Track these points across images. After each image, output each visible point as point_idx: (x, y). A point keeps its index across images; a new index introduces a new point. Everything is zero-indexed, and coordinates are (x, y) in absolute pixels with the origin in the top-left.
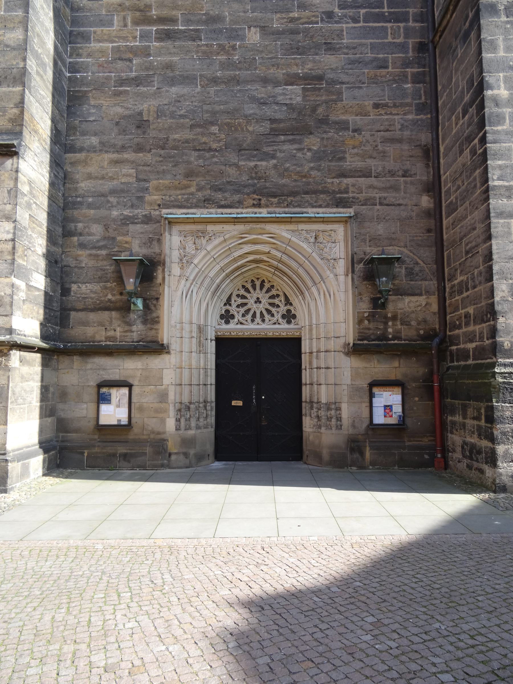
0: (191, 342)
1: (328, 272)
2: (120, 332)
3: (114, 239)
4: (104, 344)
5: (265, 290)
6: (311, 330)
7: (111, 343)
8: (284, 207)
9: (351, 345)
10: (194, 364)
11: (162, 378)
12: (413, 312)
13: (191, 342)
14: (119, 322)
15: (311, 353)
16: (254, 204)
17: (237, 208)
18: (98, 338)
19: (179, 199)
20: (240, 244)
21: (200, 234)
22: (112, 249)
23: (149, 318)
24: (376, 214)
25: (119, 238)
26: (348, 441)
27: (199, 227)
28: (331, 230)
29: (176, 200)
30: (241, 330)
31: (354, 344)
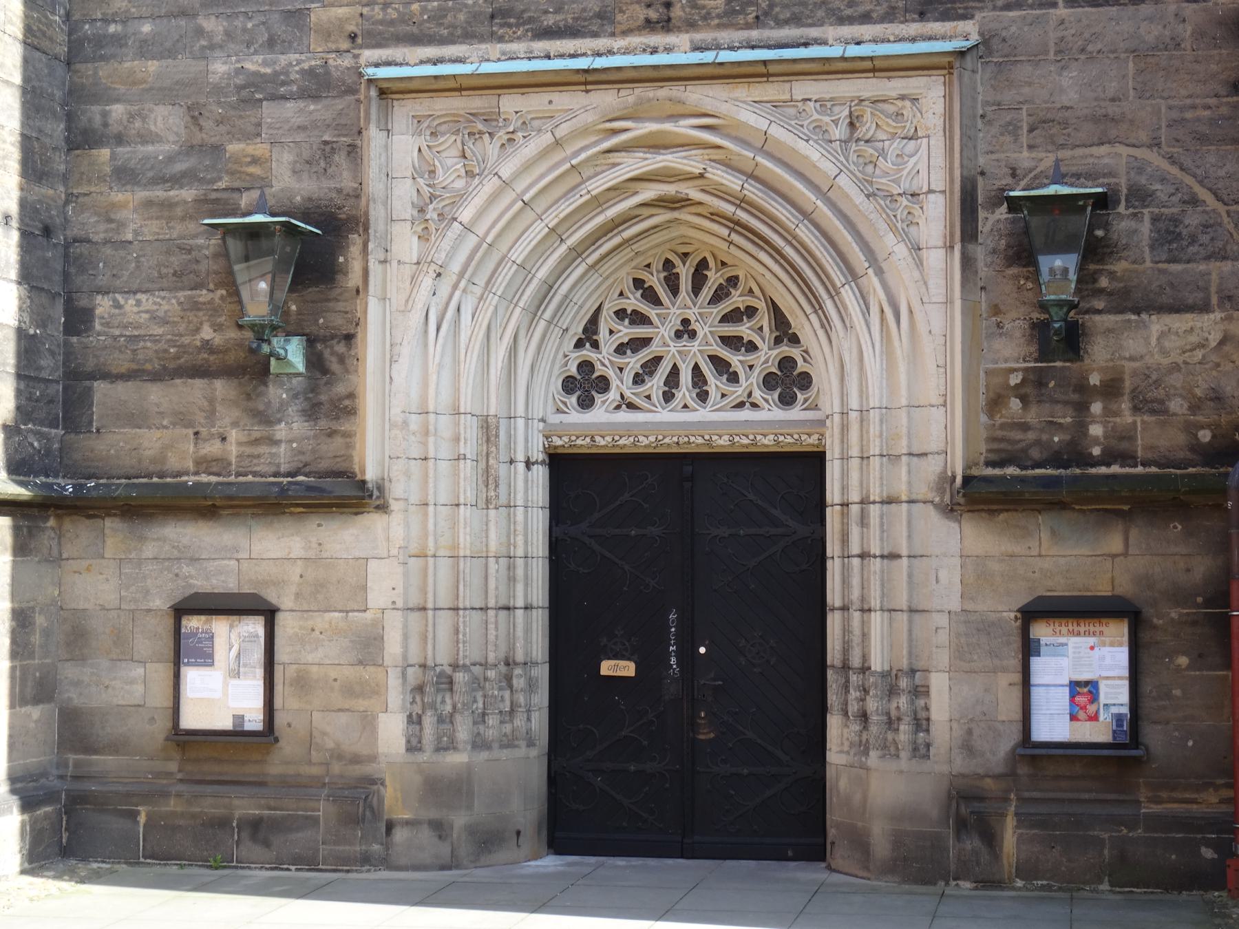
0: (456, 474)
1: (890, 239)
2: (239, 444)
3: (217, 149)
4: (190, 480)
5: (707, 292)
6: (845, 428)
7: (214, 479)
8: (748, 26)
9: (959, 480)
10: (466, 543)
11: (364, 588)
12: (1175, 367)
13: (456, 474)
14: (236, 413)
15: (845, 504)
16: (648, 21)
17: (595, 35)
18: (173, 462)
19: (412, 14)
20: (609, 151)
21: (480, 126)
22: (213, 181)
23: (323, 398)
24: (1053, 36)
25: (233, 148)
26: (950, 797)
27: (477, 103)
28: (902, 98)
29: (403, 19)
30: (628, 429)
31: (967, 480)
